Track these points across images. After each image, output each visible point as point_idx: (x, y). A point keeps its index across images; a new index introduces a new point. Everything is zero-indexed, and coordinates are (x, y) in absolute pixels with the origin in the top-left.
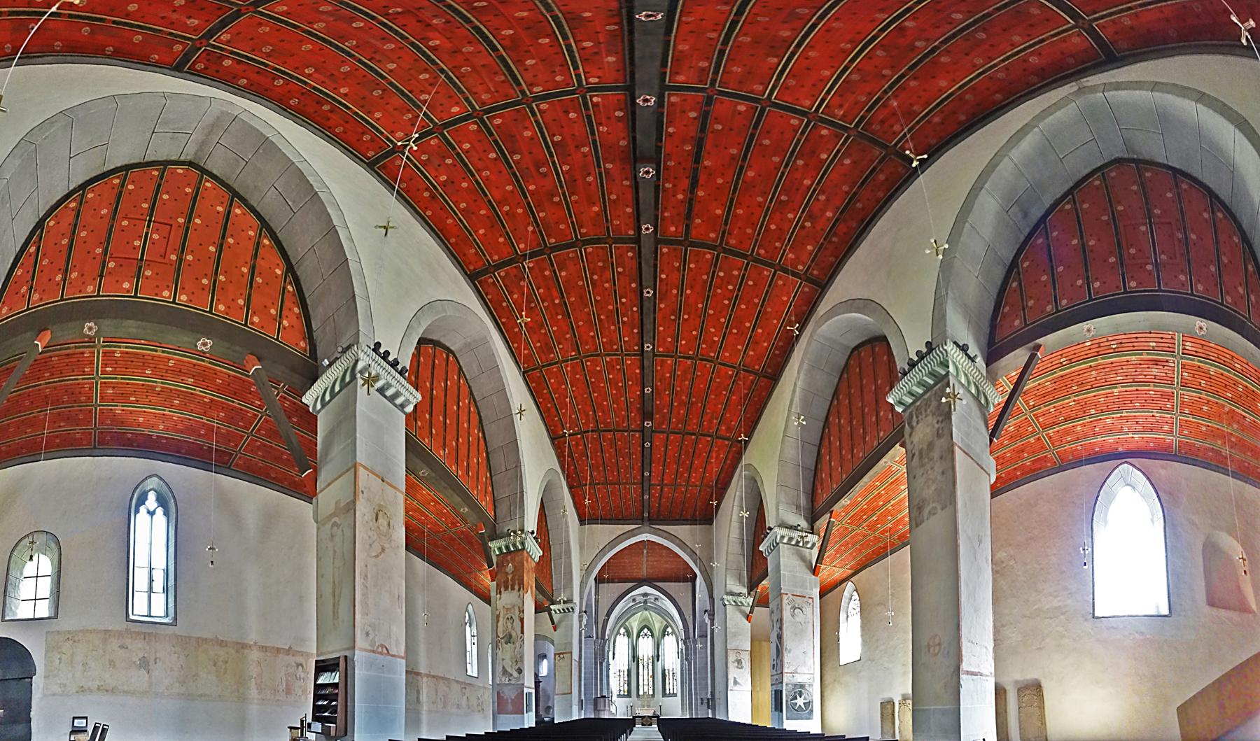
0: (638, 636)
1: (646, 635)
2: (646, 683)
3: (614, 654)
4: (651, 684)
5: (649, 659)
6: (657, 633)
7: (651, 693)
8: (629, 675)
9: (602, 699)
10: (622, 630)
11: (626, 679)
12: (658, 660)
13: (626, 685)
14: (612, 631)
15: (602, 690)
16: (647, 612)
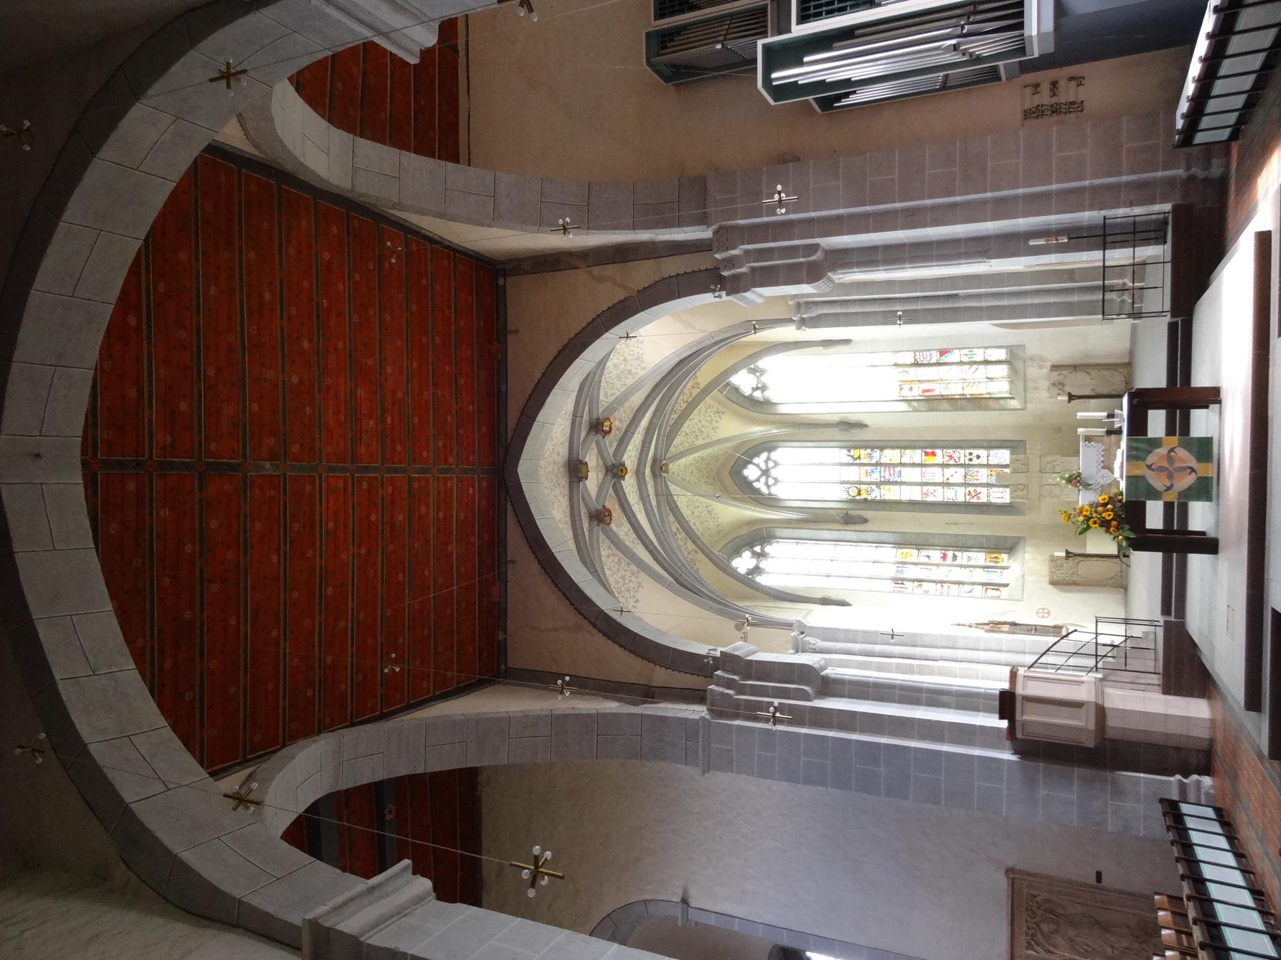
0: (770, 502)
1: (766, 473)
2: (957, 475)
3: (825, 601)
4: (961, 455)
5: (856, 462)
6: (757, 431)
7: (1003, 456)
8: (921, 543)
9: (1027, 716)
10: (743, 563)
11: (936, 555)
12: (860, 425)
13: (963, 557)
14: (720, 605)
15: (967, 700)
16: (673, 467)
